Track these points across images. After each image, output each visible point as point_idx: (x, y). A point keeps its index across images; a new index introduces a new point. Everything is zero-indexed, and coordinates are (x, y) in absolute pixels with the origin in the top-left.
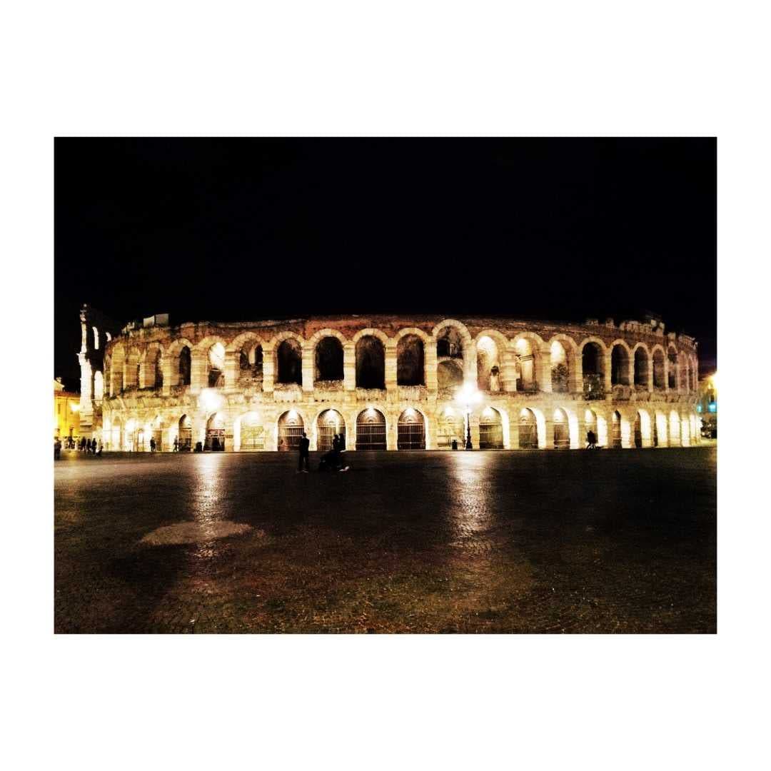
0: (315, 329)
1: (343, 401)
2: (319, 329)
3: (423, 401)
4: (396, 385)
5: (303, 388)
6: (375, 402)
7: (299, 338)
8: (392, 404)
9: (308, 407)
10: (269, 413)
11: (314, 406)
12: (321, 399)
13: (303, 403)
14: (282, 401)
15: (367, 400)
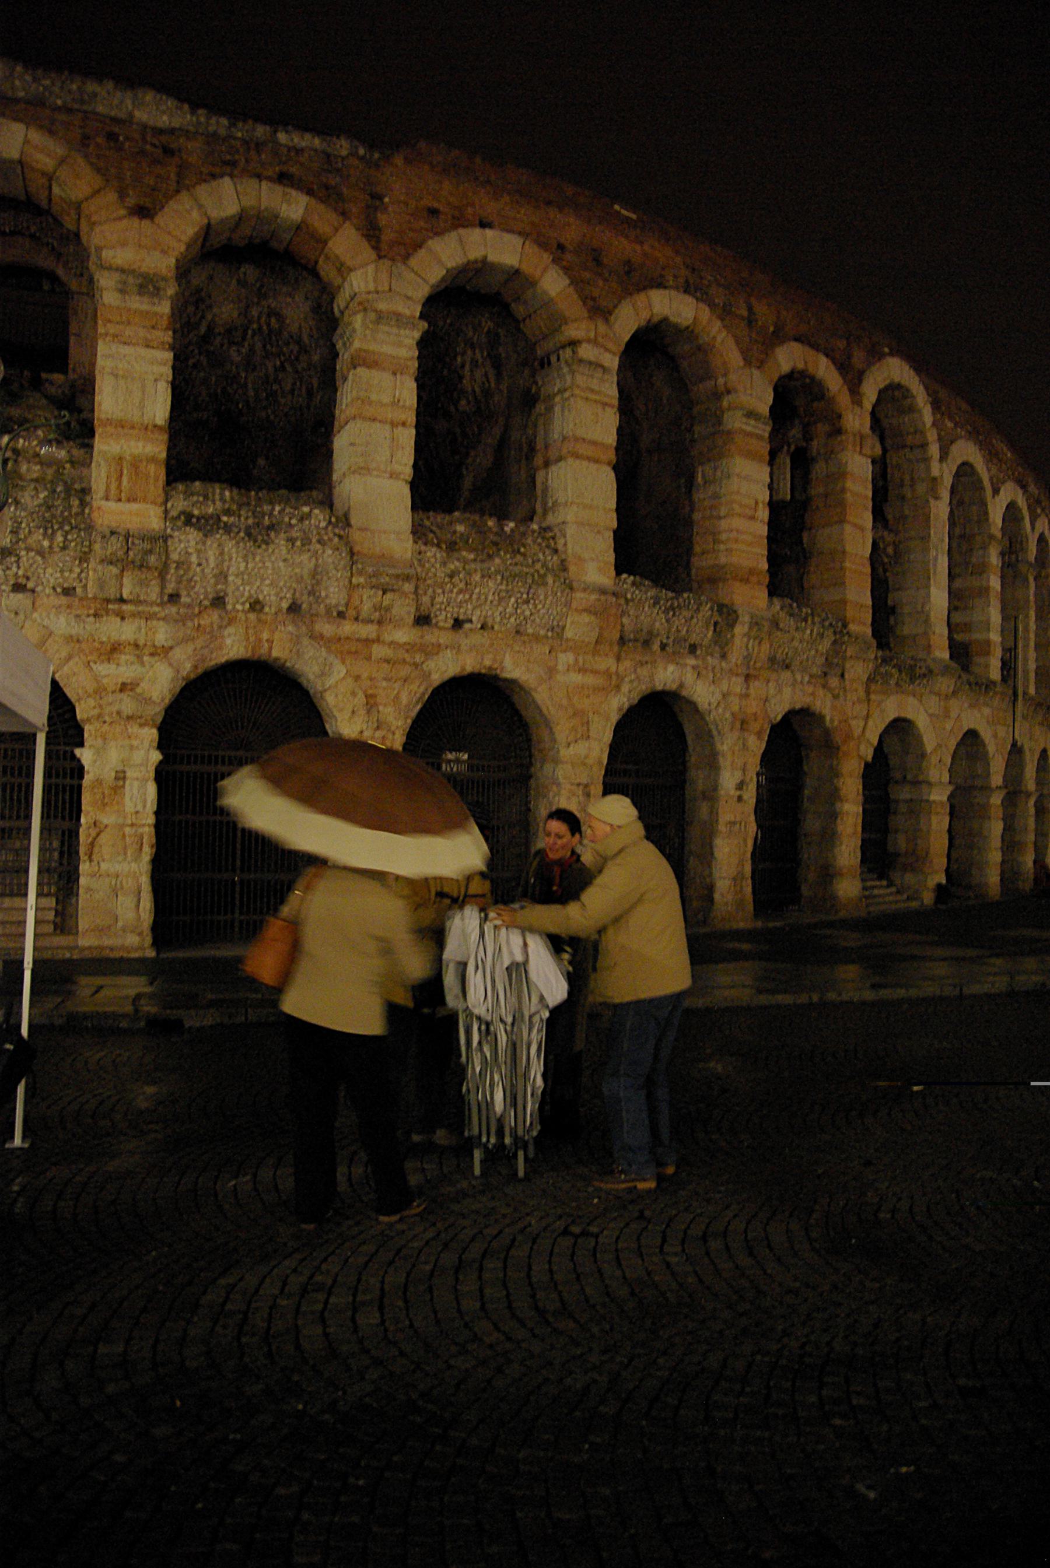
0: (433, 212)
1: (558, 631)
2: (459, 222)
3: (834, 682)
4: (764, 594)
5: (356, 536)
6: (691, 661)
7: (345, 243)
8: (747, 677)
9: (379, 651)
10: (123, 669)
11: (410, 647)
12: (453, 611)
13: (348, 628)
14: (218, 601)
15: (656, 647)
